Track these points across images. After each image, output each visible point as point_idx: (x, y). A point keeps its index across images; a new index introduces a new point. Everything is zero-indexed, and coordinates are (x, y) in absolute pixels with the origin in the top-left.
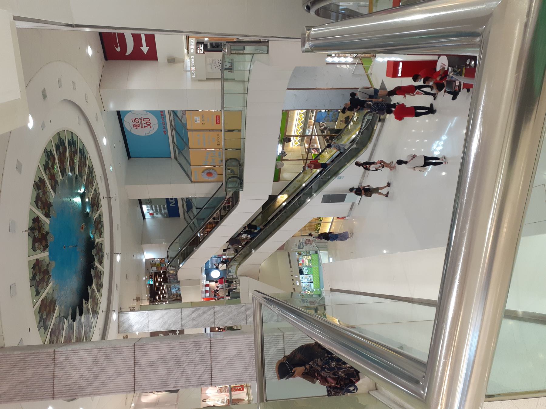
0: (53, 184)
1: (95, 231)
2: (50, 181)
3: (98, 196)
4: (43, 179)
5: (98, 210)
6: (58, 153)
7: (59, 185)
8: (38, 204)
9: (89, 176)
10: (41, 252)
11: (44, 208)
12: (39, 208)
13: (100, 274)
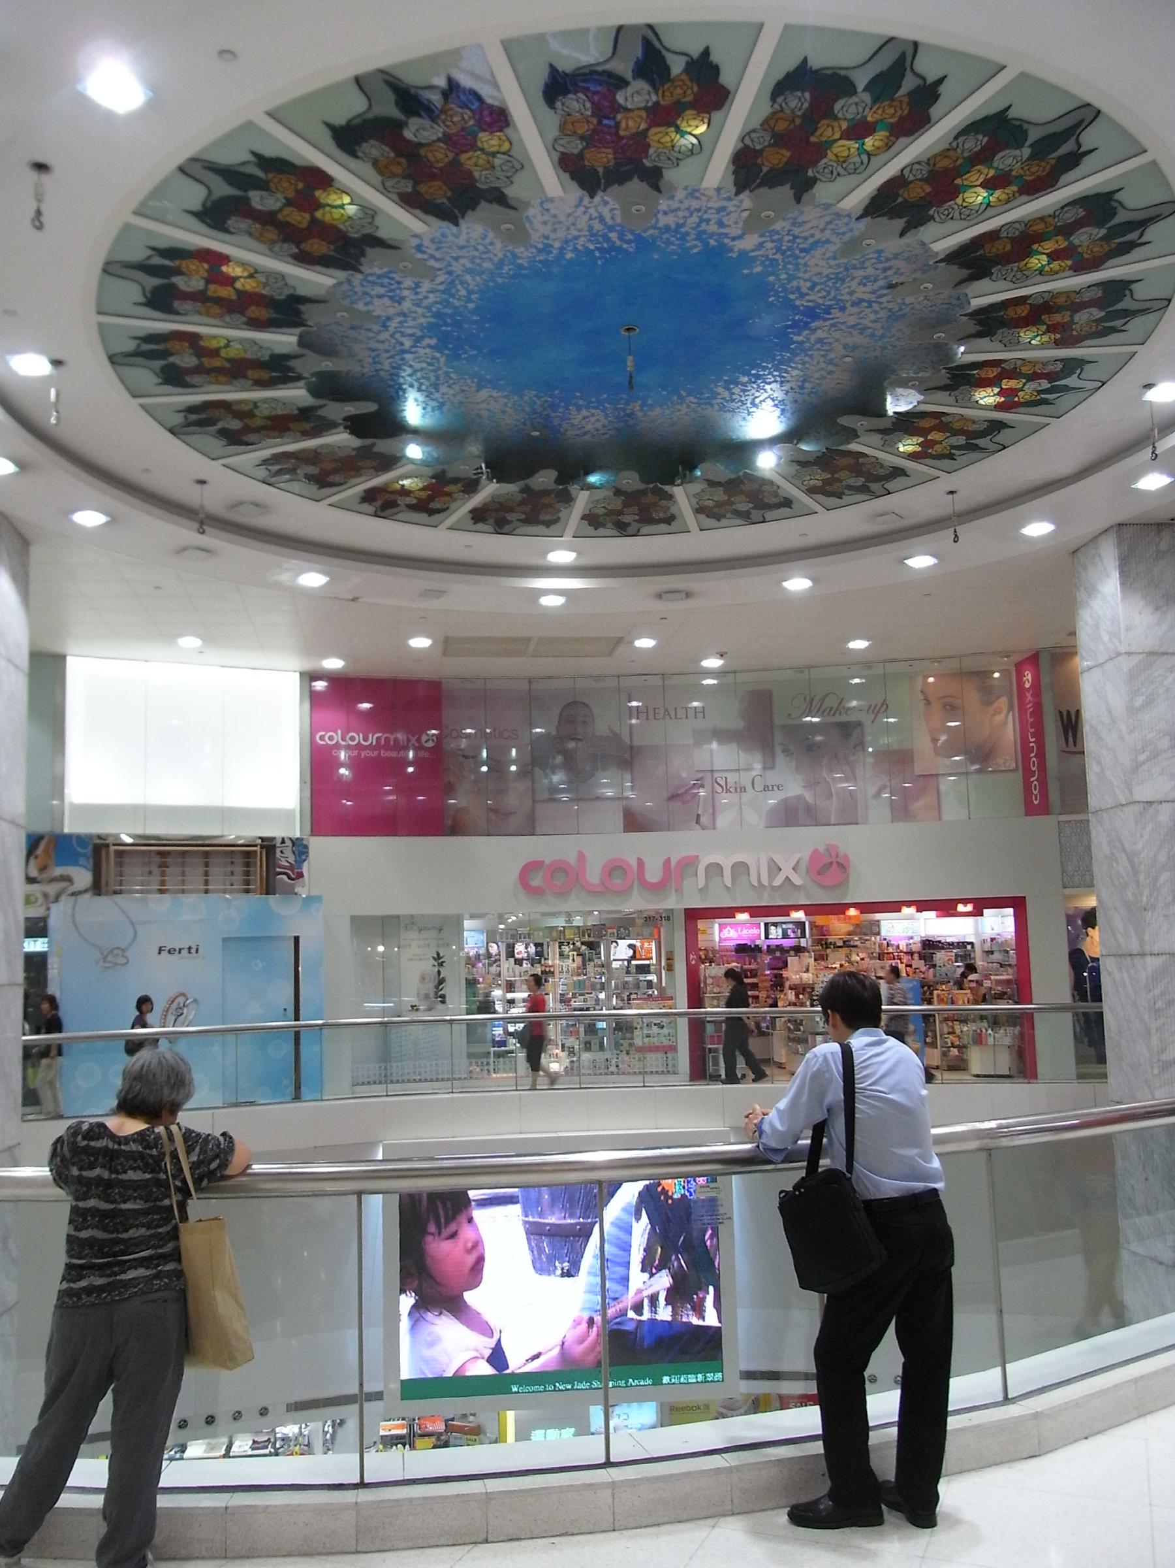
0: (917, 192)
1: (719, 484)
2: (925, 170)
3: (874, 486)
4: (935, 111)
5: (811, 491)
6: (1070, 216)
7: (902, 234)
8: (793, 89)
9: (956, 433)
10: (552, 147)
11: (779, 140)
12: (774, 97)
13: (548, 517)
